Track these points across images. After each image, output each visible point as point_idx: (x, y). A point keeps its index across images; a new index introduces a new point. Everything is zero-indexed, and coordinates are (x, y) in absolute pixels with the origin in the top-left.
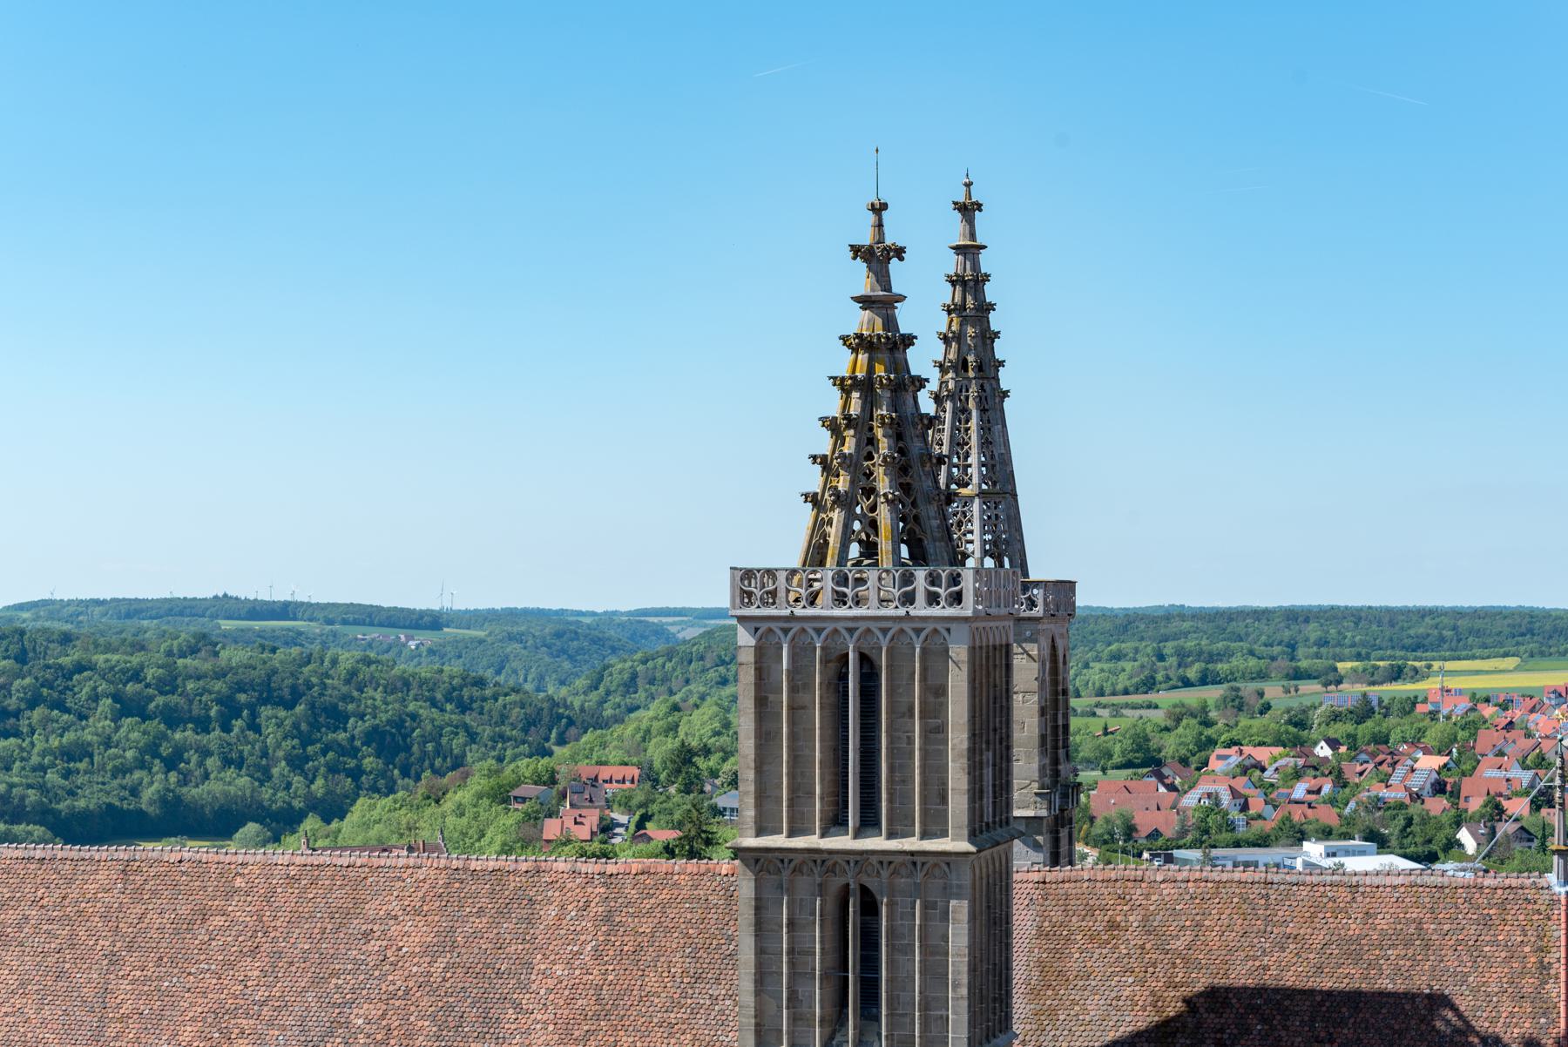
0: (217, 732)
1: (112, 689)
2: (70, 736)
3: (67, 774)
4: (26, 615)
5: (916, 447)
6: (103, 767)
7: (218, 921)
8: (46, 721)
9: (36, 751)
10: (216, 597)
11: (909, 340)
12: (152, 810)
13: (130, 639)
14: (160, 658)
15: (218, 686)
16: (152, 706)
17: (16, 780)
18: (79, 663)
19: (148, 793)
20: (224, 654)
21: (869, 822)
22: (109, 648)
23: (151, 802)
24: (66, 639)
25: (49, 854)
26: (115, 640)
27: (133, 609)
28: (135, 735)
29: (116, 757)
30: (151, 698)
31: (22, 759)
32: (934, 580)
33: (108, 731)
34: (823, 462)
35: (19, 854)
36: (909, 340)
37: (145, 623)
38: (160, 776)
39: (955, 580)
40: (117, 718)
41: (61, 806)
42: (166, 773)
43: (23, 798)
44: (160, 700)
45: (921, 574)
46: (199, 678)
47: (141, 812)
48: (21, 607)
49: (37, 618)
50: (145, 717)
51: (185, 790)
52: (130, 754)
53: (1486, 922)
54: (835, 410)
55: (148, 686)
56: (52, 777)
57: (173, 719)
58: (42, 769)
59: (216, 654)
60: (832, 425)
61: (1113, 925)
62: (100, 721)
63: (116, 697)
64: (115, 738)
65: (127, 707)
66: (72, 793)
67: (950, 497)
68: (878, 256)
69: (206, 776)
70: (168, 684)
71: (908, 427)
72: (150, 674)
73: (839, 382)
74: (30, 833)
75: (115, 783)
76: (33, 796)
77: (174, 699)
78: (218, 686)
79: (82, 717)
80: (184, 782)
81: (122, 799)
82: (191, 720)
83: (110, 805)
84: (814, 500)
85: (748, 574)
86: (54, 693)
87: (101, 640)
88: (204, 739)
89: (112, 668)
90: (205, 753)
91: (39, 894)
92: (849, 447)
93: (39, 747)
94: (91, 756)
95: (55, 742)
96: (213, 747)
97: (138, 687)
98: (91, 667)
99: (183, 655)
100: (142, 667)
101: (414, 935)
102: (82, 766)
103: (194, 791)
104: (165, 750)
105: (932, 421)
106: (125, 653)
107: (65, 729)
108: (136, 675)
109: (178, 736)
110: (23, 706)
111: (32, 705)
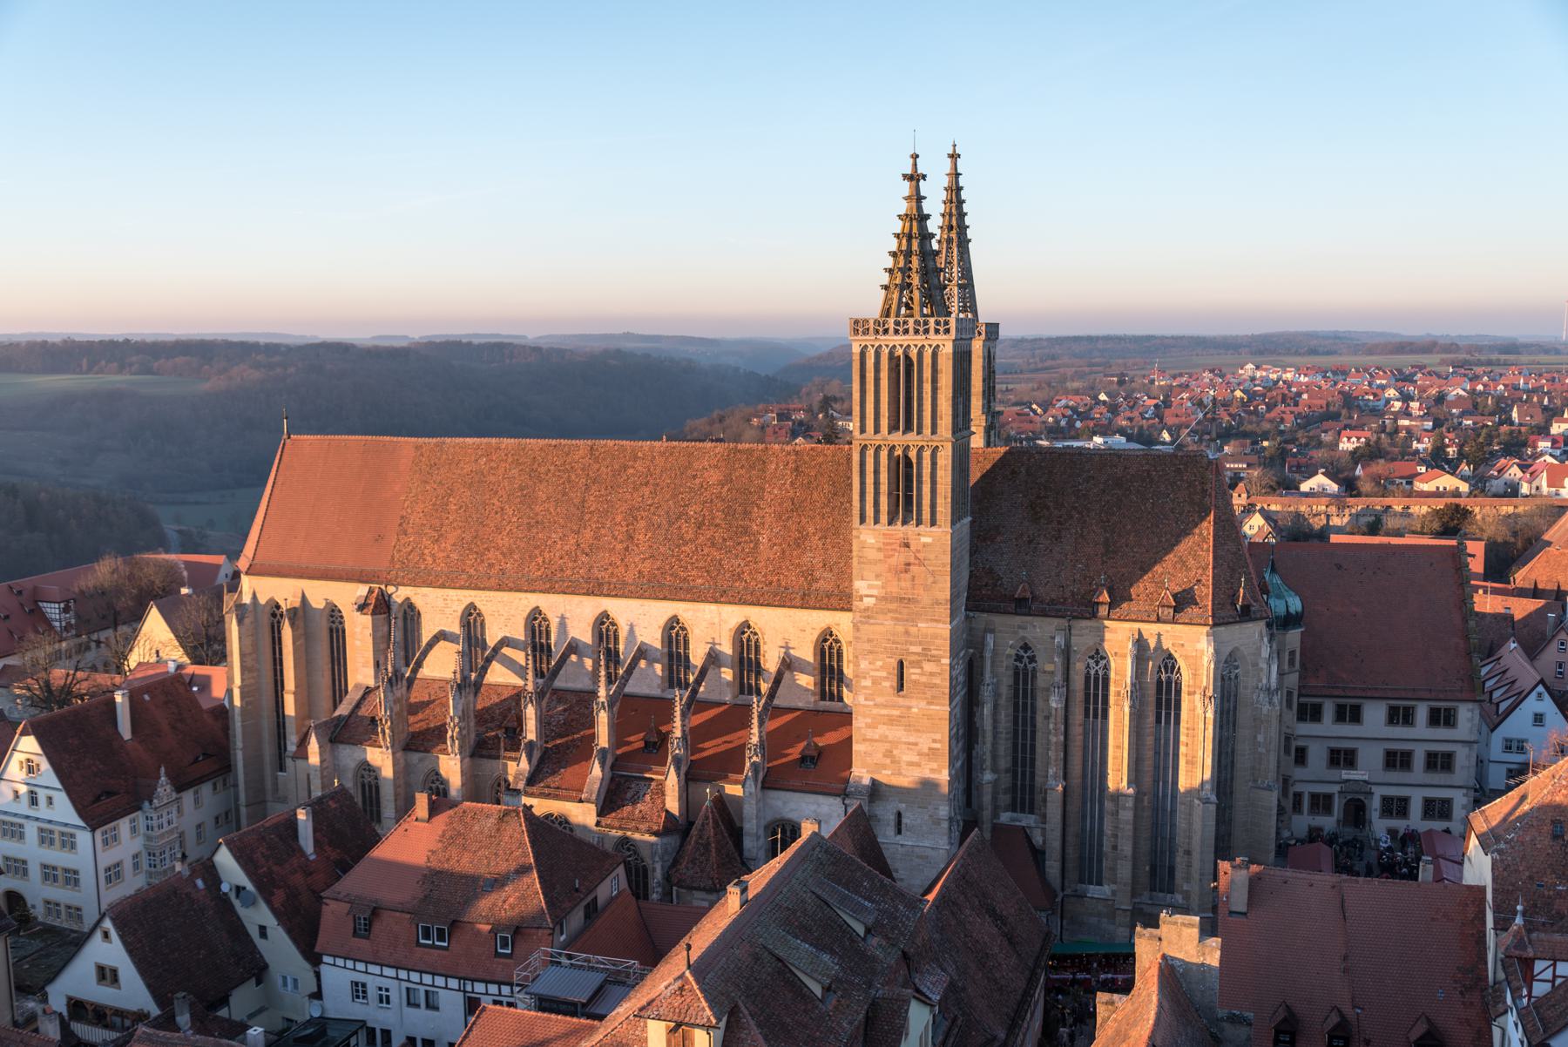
5: (931, 264)
7: (631, 471)
11: (928, 217)
21: (908, 428)
32: (938, 323)
34: (890, 271)
36: (928, 217)
39: (946, 323)
45: (932, 320)
53: (1178, 471)
54: (894, 248)
60: (894, 254)
61: (1013, 472)
67: (945, 287)
68: (915, 178)
71: (927, 255)
73: (897, 236)
84: (886, 288)
85: (856, 322)
92: (901, 264)
101: (714, 477)
105: (938, 253)
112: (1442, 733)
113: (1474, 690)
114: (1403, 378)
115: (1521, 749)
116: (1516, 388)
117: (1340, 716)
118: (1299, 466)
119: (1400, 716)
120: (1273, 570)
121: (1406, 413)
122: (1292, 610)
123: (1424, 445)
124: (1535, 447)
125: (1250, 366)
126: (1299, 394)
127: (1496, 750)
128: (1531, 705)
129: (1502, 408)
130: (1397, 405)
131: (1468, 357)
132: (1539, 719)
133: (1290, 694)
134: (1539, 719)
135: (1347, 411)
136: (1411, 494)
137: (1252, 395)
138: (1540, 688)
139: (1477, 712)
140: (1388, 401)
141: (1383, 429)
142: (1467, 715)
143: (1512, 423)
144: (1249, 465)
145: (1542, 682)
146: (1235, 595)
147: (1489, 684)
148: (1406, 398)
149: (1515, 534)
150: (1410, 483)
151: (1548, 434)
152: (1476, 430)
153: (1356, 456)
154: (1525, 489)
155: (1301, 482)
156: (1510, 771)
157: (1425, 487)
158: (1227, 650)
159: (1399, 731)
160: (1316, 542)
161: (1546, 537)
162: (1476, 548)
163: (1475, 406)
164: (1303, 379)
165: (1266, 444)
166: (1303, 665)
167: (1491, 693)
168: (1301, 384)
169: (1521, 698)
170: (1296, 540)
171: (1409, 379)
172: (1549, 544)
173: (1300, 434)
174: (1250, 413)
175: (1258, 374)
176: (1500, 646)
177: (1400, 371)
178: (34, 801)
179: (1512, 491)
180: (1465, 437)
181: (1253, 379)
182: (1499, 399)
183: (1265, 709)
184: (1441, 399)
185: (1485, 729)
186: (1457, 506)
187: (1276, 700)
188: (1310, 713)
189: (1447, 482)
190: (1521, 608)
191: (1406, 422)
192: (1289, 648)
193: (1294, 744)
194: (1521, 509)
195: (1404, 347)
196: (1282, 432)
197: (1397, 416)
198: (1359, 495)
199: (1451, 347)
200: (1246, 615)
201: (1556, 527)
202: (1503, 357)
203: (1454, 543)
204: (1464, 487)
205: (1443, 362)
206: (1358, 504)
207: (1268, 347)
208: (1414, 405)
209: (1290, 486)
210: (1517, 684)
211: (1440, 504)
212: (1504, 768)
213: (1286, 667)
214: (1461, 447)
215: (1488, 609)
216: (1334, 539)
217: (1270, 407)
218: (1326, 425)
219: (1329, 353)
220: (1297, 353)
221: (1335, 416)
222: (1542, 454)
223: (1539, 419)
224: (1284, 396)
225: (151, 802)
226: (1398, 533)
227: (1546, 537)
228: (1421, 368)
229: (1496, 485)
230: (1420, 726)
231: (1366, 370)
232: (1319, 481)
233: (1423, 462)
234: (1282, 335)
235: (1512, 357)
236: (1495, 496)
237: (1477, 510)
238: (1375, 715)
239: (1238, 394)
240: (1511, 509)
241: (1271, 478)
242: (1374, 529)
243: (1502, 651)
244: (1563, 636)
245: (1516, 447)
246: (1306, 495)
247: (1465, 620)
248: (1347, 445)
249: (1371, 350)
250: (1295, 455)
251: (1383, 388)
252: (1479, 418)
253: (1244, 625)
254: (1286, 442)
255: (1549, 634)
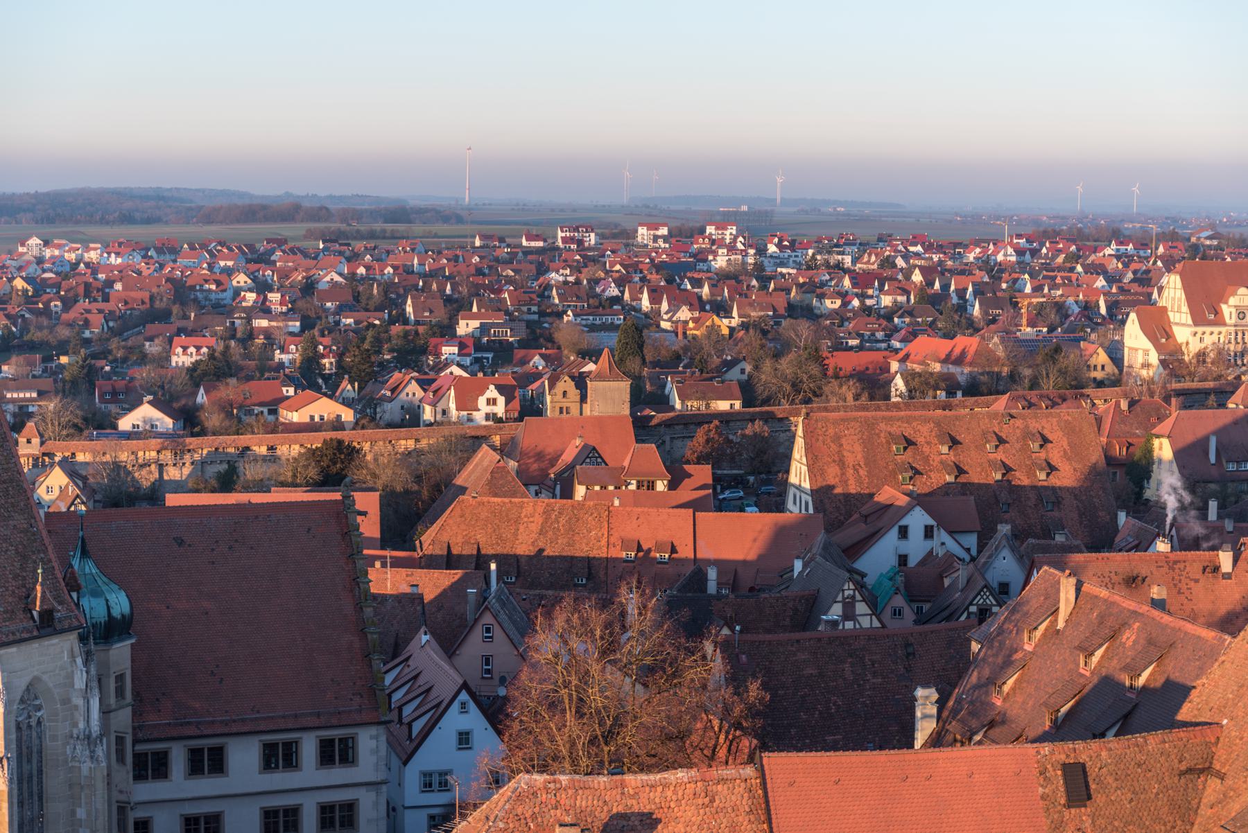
112: (338, 774)
113: (376, 707)
114: (256, 258)
115: (444, 786)
116: (409, 271)
117: (195, 768)
118: (115, 393)
119: (279, 756)
120: (85, 553)
121: (265, 311)
122: (116, 613)
123: (289, 356)
124: (438, 354)
125: (34, 241)
126: (110, 283)
127: (412, 792)
128: (454, 721)
129: (391, 300)
130: (251, 297)
131: (343, 226)
132: (464, 739)
133: (120, 740)
134: (464, 739)
135: (181, 306)
136: (275, 428)
137: (40, 286)
138: (464, 696)
139: (383, 738)
140: (237, 292)
141: (232, 333)
142: (370, 744)
143: (406, 321)
144: (40, 394)
145: (465, 686)
146: (29, 596)
147: (397, 696)
148: (262, 288)
149: (418, 479)
150: (273, 412)
151: (453, 335)
152: (359, 333)
153: (196, 375)
154: (428, 414)
155: (119, 416)
156: (432, 817)
157: (295, 417)
158: (21, 683)
159: (281, 779)
160: (145, 507)
161: (459, 481)
162: (368, 503)
163: (357, 298)
164: (114, 260)
165: (64, 360)
166: (137, 694)
167: (400, 709)
168: (111, 268)
169: (439, 711)
170: (116, 505)
171: (263, 259)
172: (463, 490)
173: (114, 344)
174: (38, 313)
175: (48, 253)
176: (408, 641)
177: (251, 247)
179: (411, 418)
180: (346, 342)
181: (40, 261)
182: (387, 287)
183: (86, 767)
184: (309, 287)
185: (395, 762)
186: (340, 442)
187: (100, 752)
188: (151, 766)
189: (324, 408)
190: (432, 584)
191: (264, 323)
192: (115, 669)
193: (132, 816)
194: (424, 443)
195: (254, 212)
196: (87, 342)
197: (250, 313)
198: (203, 433)
199: (319, 213)
200: (47, 625)
201: (470, 467)
202: (389, 227)
203: (337, 496)
204: (348, 415)
205: (310, 235)
206: (202, 447)
207: (62, 211)
208: (274, 297)
209: (101, 424)
210: (433, 694)
211: (316, 441)
212: (423, 816)
213: (112, 700)
214: (340, 356)
215: (389, 589)
216: (172, 500)
217: (68, 304)
218: (152, 328)
219: (149, 221)
220: (104, 221)
221: (163, 316)
222: (447, 364)
223: (441, 314)
224: (87, 286)
226: (261, 486)
227: (459, 481)
228: (281, 242)
229: (390, 410)
230: (309, 771)
231: (204, 246)
232: (145, 414)
233: (290, 380)
234: (80, 193)
235: (401, 227)
236: (390, 425)
237: (367, 446)
238: (244, 757)
239: (19, 283)
240: (411, 444)
241: (74, 412)
242: (227, 482)
243: (413, 647)
244: (488, 619)
245: (413, 355)
246: (128, 436)
247: (359, 608)
248: (182, 358)
249: (209, 217)
250: (108, 377)
251: (229, 272)
252: (362, 315)
253: (46, 642)
254: (95, 356)
255: (470, 617)
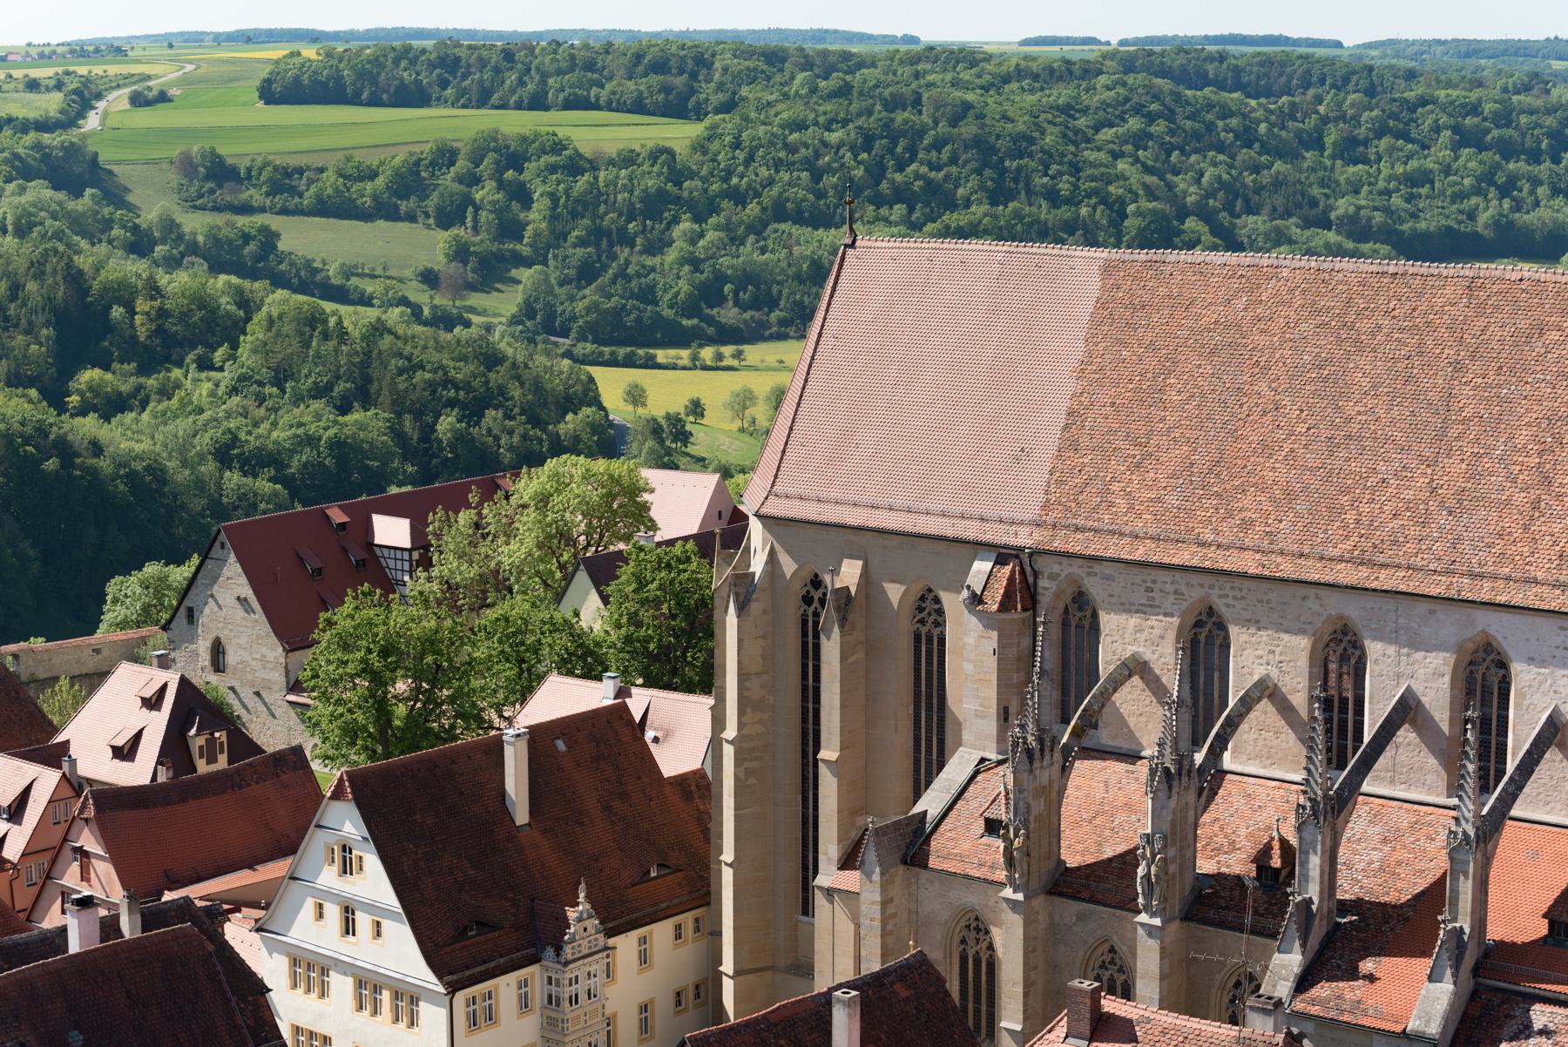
0: (1547, 164)
1: (1452, 121)
2: (1413, 164)
3: (1410, 198)
4: (1374, 53)
6: (1443, 193)
8: (1391, 150)
9: (1382, 176)
10: (1548, 39)
12: (1488, 233)
13: (1469, 76)
14: (1496, 93)
15: (1549, 121)
16: (1489, 137)
17: (1363, 202)
18: (1422, 97)
19: (1484, 218)
20: (1555, 92)
22: (1449, 84)
23: (1486, 226)
24: (1411, 75)
25: (1401, 270)
26: (1455, 77)
27: (1472, 49)
28: (1472, 164)
29: (1456, 184)
30: (1488, 131)
31: (1370, 184)
33: (1448, 160)
35: (1374, 268)
37: (1483, 62)
38: (1495, 202)
40: (1456, 147)
41: (1406, 227)
42: (1500, 200)
43: (1370, 219)
44: (1495, 133)
46: (1532, 114)
47: (1476, 235)
48: (1370, 46)
49: (1384, 56)
50: (1482, 148)
51: (1517, 215)
52: (1467, 182)
55: (1485, 119)
56: (1396, 201)
57: (1508, 150)
58: (1387, 193)
59: (1548, 92)
62: (1442, 151)
63: (1456, 129)
64: (1455, 166)
65: (1464, 139)
66: (1414, 216)
69: (1537, 204)
70: (1505, 118)
72: (1488, 108)
74: (1376, 251)
75: (1455, 207)
76: (1378, 217)
77: (1508, 132)
78: (1549, 121)
79: (1425, 147)
80: (1518, 206)
81: (1460, 222)
82: (1523, 153)
83: (1449, 228)
86: (1400, 123)
87: (1443, 77)
88: (1536, 169)
89: (1452, 103)
90: (1536, 182)
91: (1392, 306)
93: (1385, 172)
94: (1432, 182)
95: (1400, 169)
96: (1544, 176)
97: (1476, 120)
98: (1434, 101)
99: (1517, 92)
100: (1480, 101)
102: (1424, 191)
103: (1526, 217)
104: (1501, 179)
106: (1465, 89)
107: (1409, 157)
108: (1475, 109)
109: (1511, 166)
110: (1371, 135)
111: (1379, 136)
178: (349, 928)
225: (558, 950)
